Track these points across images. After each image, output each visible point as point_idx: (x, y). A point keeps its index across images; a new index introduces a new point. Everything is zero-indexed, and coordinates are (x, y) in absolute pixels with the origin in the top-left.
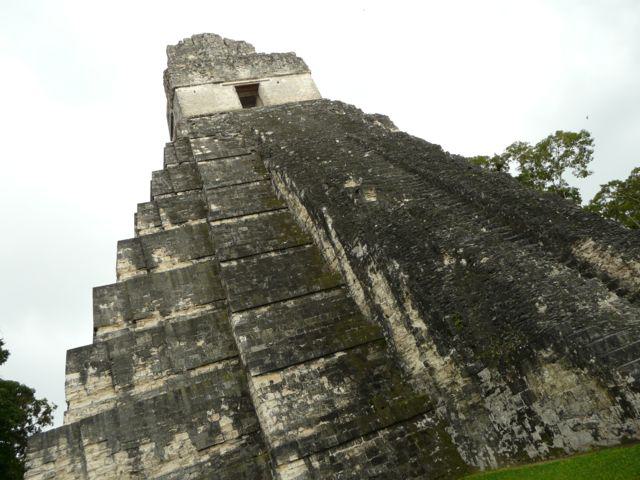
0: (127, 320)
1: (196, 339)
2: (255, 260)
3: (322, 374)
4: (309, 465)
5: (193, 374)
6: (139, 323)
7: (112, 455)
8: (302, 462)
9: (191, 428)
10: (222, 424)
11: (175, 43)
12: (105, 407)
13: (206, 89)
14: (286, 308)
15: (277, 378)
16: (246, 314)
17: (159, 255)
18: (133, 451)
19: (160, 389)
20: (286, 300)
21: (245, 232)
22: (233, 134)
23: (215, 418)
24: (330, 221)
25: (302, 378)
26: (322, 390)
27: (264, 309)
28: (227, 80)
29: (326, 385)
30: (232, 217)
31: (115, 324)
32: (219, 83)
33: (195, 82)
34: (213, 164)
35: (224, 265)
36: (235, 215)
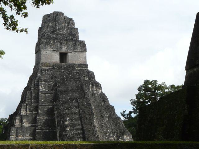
2: (43, 131)
13: (50, 52)
17: (24, 121)
24: (59, 130)
30: (42, 117)
34: (43, 95)
35: (37, 130)
36: (43, 116)
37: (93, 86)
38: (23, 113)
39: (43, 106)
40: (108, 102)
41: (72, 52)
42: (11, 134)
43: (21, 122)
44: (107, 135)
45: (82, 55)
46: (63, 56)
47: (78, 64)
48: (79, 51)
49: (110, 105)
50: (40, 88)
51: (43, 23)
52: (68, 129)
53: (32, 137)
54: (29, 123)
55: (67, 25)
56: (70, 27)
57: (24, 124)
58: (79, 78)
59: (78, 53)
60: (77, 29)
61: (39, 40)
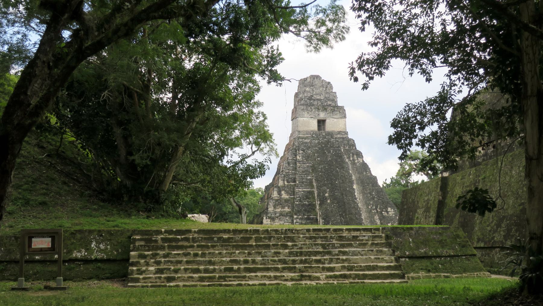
17: (283, 192)
28: (316, 117)
37: (353, 155)
38: (281, 183)
40: (370, 172)
43: (279, 193)
45: (341, 121)
46: (321, 123)
50: (298, 158)
52: (329, 201)
55: (324, 89)
57: (283, 196)
58: (339, 147)
60: (335, 93)
61: (295, 107)
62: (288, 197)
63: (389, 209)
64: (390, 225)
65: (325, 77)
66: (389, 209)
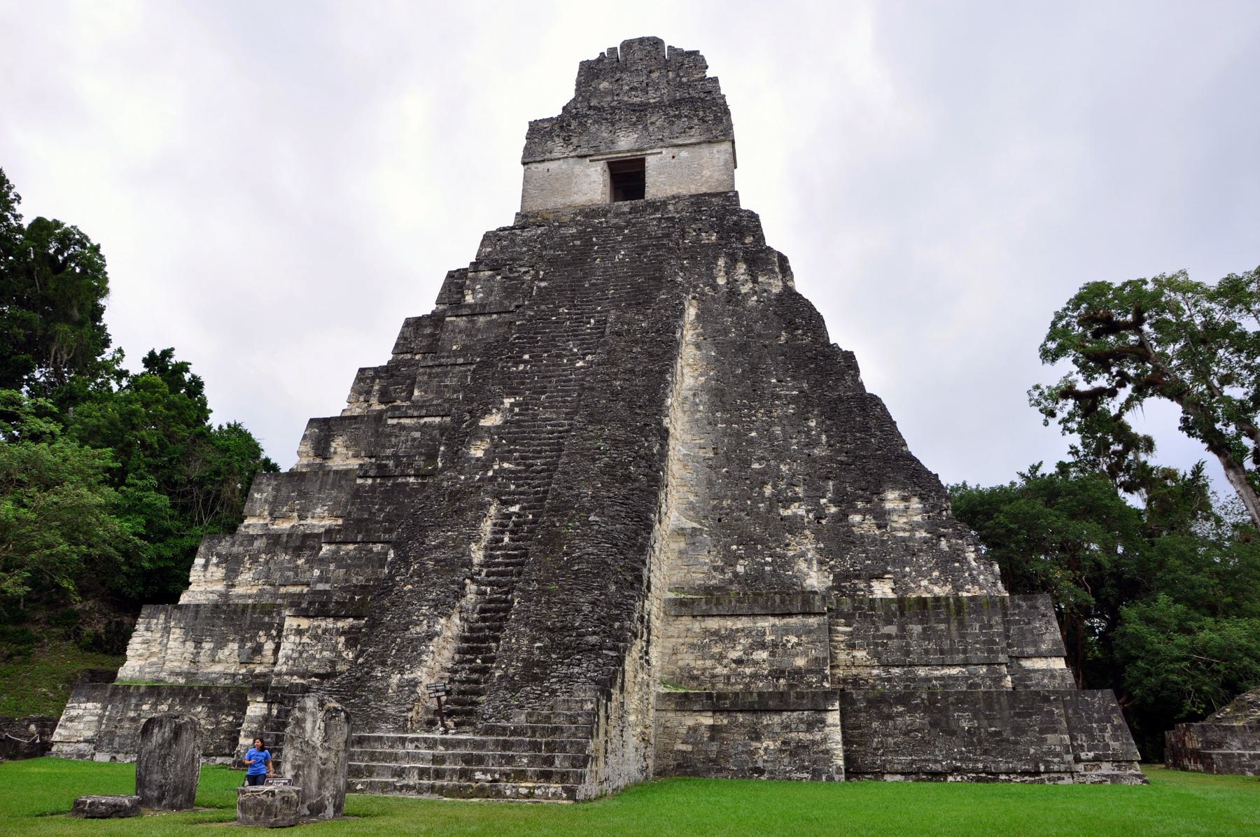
0: (271, 514)
1: (299, 556)
3: (344, 633)
4: (270, 709)
5: (283, 590)
6: (279, 522)
7: (184, 642)
8: (266, 705)
9: (242, 642)
10: (266, 647)
11: (594, 56)
12: (210, 596)
14: (371, 551)
15: (305, 623)
16: (333, 547)
17: (338, 444)
18: (198, 643)
19: (250, 596)
20: (374, 543)
21: (414, 439)
22: (523, 269)
23: (263, 639)
25: (325, 631)
26: (334, 649)
27: (351, 547)
28: (598, 152)
29: (340, 646)
30: (412, 417)
31: (260, 516)
32: (585, 156)
33: (556, 155)
34: (462, 322)
35: (359, 481)
36: (416, 414)
37: (733, 260)
39: (440, 365)
41: (664, 151)
42: (248, 505)
44: (768, 490)
47: (691, 196)
48: (693, 140)
49: (826, 343)
50: (469, 299)
51: (579, 84)
52: (477, 452)
53: (340, 522)
54: (355, 456)
56: (684, 80)
59: (690, 149)
60: (715, 80)
62: (354, 463)
63: (892, 499)
64: (883, 589)
65: (677, 39)
66: (892, 499)
